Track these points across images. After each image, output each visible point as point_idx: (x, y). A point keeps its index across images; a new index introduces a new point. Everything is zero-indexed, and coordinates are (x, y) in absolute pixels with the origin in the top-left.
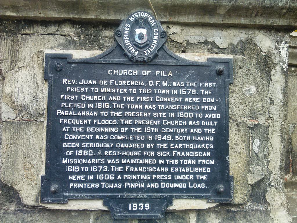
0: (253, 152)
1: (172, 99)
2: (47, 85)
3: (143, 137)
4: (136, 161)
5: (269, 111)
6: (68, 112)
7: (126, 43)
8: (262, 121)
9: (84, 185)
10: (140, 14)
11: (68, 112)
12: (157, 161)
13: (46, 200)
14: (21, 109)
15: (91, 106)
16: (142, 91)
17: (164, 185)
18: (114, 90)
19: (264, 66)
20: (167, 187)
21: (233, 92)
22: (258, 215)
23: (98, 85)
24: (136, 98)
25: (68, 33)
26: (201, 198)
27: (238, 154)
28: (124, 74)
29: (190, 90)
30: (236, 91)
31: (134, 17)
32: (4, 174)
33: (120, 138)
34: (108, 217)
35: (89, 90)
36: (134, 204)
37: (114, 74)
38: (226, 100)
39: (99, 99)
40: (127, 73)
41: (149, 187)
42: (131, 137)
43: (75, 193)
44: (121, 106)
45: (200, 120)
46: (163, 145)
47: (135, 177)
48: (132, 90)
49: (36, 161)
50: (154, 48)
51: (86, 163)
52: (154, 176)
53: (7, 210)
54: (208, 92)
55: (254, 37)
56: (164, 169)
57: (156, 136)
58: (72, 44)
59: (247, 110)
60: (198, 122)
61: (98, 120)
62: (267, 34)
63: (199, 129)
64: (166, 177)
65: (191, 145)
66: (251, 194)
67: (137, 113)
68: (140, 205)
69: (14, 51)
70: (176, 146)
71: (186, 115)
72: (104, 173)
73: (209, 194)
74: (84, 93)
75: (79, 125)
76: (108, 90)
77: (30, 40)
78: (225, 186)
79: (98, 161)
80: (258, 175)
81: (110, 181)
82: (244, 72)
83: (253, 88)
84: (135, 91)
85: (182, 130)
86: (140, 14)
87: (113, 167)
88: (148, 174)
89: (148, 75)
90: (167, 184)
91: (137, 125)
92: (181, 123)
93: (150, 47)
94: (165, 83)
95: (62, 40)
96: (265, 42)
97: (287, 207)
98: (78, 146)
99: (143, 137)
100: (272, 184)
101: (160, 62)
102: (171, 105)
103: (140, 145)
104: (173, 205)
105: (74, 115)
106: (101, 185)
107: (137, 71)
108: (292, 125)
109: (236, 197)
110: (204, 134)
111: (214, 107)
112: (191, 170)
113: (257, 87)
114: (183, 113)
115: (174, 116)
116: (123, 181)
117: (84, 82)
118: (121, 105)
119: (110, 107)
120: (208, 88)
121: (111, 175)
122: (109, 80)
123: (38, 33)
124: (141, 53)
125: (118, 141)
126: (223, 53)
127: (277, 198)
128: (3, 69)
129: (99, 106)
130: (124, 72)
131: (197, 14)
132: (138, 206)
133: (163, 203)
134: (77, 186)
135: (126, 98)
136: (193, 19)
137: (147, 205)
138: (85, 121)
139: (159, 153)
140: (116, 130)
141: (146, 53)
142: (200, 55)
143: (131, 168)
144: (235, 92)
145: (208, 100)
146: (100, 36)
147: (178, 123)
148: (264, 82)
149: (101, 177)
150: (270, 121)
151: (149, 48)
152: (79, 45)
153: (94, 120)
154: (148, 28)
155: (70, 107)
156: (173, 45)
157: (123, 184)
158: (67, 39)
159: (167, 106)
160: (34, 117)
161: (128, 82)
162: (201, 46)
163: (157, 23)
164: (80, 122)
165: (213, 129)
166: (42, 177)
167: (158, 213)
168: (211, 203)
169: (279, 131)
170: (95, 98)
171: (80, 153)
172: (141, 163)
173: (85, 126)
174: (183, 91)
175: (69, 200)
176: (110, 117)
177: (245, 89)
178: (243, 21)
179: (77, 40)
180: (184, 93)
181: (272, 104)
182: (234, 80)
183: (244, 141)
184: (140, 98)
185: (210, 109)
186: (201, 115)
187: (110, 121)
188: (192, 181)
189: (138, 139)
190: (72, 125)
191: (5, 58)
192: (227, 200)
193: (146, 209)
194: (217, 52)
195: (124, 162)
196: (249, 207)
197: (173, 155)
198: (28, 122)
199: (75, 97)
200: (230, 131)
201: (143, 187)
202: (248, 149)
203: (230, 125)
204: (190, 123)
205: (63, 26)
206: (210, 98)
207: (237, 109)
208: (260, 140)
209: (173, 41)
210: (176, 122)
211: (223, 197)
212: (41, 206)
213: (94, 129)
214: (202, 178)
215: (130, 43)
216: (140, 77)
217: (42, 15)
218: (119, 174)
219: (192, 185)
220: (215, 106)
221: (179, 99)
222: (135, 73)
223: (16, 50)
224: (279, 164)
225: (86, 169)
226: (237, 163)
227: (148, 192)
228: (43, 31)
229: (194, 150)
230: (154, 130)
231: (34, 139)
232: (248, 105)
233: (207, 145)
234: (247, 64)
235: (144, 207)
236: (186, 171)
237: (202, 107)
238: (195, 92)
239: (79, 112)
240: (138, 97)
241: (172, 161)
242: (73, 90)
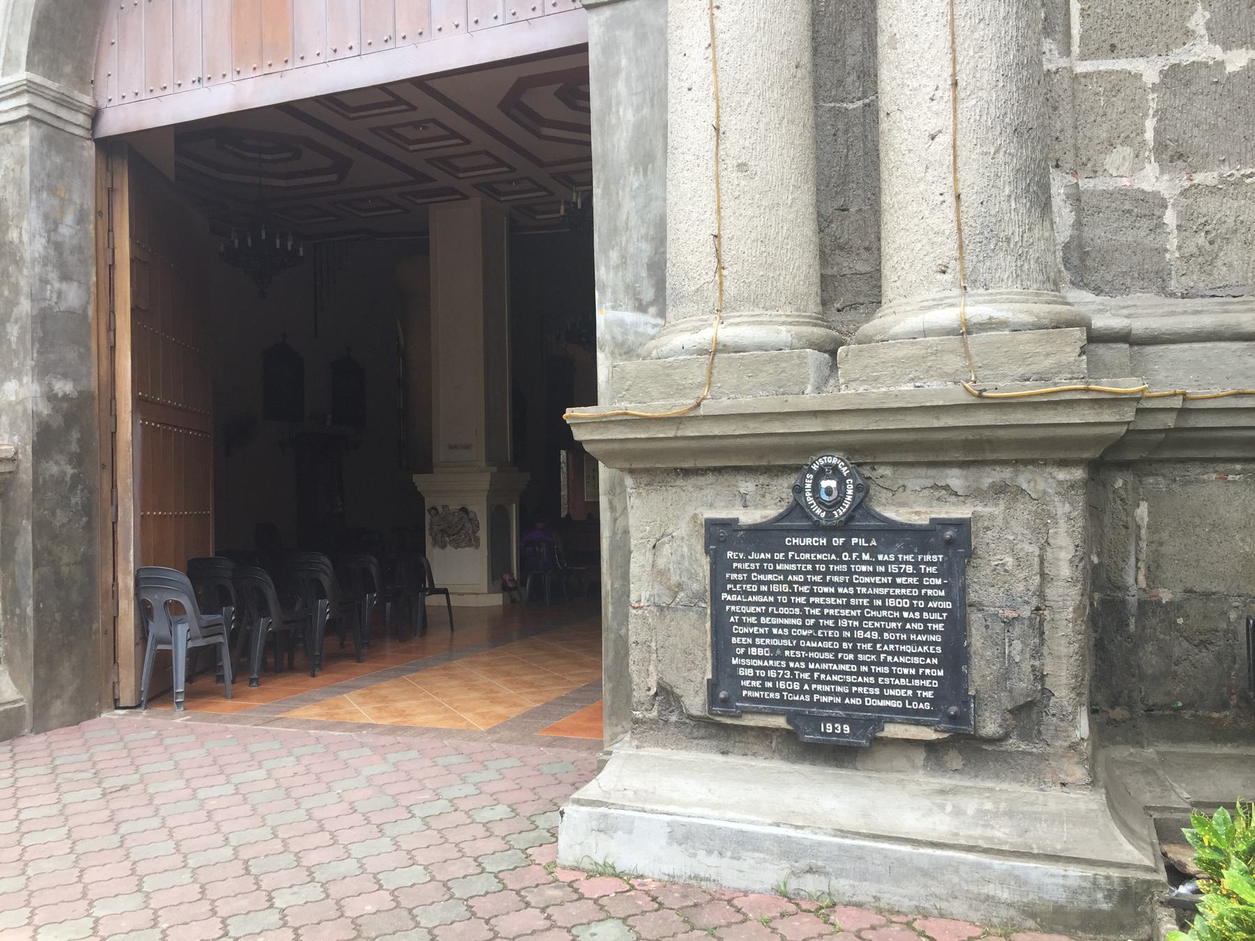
15: (764, 588)
17: (870, 702)
18: (793, 567)
33: (804, 633)
44: (805, 589)
45: (921, 611)
47: (827, 688)
52: (854, 689)
54: (932, 570)
60: (917, 614)
70: (886, 648)
75: (751, 615)
76: (787, 567)
81: (793, 691)
84: (823, 568)
85: (893, 625)
91: (828, 617)
106: (782, 696)
110: (926, 631)
116: (812, 693)
117: (754, 556)
124: (830, 515)
125: (802, 637)
130: (808, 541)
138: (758, 610)
140: (798, 622)
149: (782, 685)
157: (812, 698)
164: (752, 609)
170: (770, 577)
171: (753, 651)
173: (758, 615)
174: (893, 568)
176: (790, 604)
186: (921, 604)
190: (742, 614)
195: (811, 666)
204: (906, 615)
210: (884, 613)
216: (829, 548)
219: (910, 704)
229: (913, 655)
241: (880, 669)
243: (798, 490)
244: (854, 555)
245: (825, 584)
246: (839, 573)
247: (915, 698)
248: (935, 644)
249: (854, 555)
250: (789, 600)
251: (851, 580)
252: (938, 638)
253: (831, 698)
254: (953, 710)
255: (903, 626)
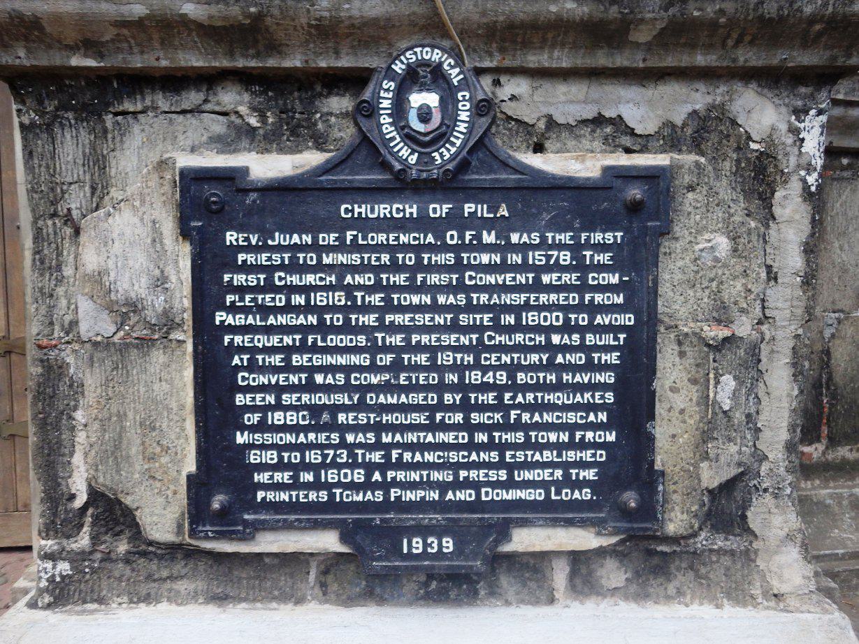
0: (717, 407)
1: (508, 279)
2: (186, 249)
3: (434, 378)
4: (419, 437)
5: (763, 300)
6: (243, 316)
7: (385, 131)
8: (743, 328)
9: (291, 496)
10: (422, 52)
11: (243, 316)
12: (471, 437)
13: (202, 531)
14: (127, 310)
15: (298, 300)
16: (430, 259)
17: (488, 494)
18: (355, 259)
19: (754, 179)
20: (496, 498)
21: (670, 254)
22: (726, 561)
23: (315, 247)
24: (412, 279)
25: (232, 106)
26: (583, 524)
27: (677, 414)
28: (382, 216)
29: (555, 253)
30: (678, 251)
31: (405, 62)
32: (97, 470)
33: (375, 380)
34: (352, 567)
35: (294, 259)
36: (415, 540)
37: (356, 216)
38: (650, 277)
39: (319, 283)
40: (391, 212)
41: (450, 500)
42: (403, 376)
43: (271, 515)
45: (582, 330)
46: (485, 397)
47: (414, 476)
48: (404, 258)
49: (173, 437)
50: (458, 143)
51: (294, 442)
52: (463, 474)
53: (109, 553)
54: (604, 258)
55: (731, 100)
56: (490, 457)
57: (467, 373)
58: (240, 136)
59: (706, 300)
60: (576, 337)
61: (319, 337)
62: (766, 91)
63: (578, 355)
64: (493, 475)
65: (557, 394)
66: (710, 510)
67: (417, 317)
68: (429, 541)
69: (98, 160)
70: (520, 399)
71: (545, 318)
72: (340, 467)
73: (601, 515)
74: (282, 267)
76: (342, 259)
77: (136, 129)
78: (641, 495)
79: (322, 438)
80: (729, 465)
82: (700, 199)
83: (723, 243)
85: (534, 358)
86: (422, 52)
87: (360, 452)
88: (449, 468)
89: (444, 215)
90: (496, 491)
91: (419, 348)
92: (531, 339)
93: (448, 141)
94: (489, 234)
95: (218, 126)
96: (760, 115)
97: (803, 542)
98: (273, 403)
99: (434, 378)
100: (764, 486)
101: (476, 180)
102: (506, 293)
103: (426, 398)
104: (511, 540)
105: (259, 323)
106: (332, 496)
107: (415, 206)
108: (833, 315)
109: (671, 520)
110: (590, 366)
111: (618, 296)
112: (557, 457)
113: (734, 239)
114: (536, 313)
115: (513, 323)
116: (386, 486)
117: (278, 239)
118: (377, 296)
119: (349, 303)
120: (601, 248)
121: (356, 471)
122: (342, 232)
123: (155, 108)
124: (426, 159)
125: (371, 388)
126: (644, 150)
127: (777, 520)
128: (73, 206)
129: (321, 301)
130: (383, 210)
131: (575, 47)
132: (426, 545)
133: (487, 536)
134: (274, 497)
135: (388, 279)
136: (562, 59)
137: (448, 542)
138: (288, 340)
139: (476, 418)
140: (362, 360)
141: (438, 157)
142: (582, 159)
143: (405, 454)
144: (673, 256)
145: (604, 278)
146: (316, 112)
147: (524, 340)
148: (753, 224)
149: (331, 476)
150: (764, 328)
151: (447, 145)
152: (264, 139)
153: (310, 337)
154: (444, 90)
155: (247, 304)
156: (510, 130)
158: (233, 122)
159: (495, 296)
160: (160, 329)
161: (392, 237)
162: (586, 131)
163: (468, 76)
164: (274, 341)
165: (614, 354)
166: (189, 477)
167: (475, 560)
168: (605, 535)
169: (788, 352)
170: (310, 279)
171: (278, 418)
172: (430, 443)
173: (288, 351)
174: (537, 258)
175: (257, 530)
176: (347, 328)
177: (701, 246)
178: (701, 59)
179: (259, 125)
180: (541, 260)
181: (772, 283)
182: (672, 221)
183: (694, 381)
184: (425, 278)
185: (606, 303)
187: (349, 337)
188: (559, 486)
189: (421, 382)
190: (253, 351)
191: (75, 179)
192: (647, 529)
193: (445, 550)
194: (628, 145)
195: (386, 439)
196: (704, 542)
197: (512, 422)
198: (145, 344)
199: (258, 279)
200: (659, 356)
201: (437, 498)
202: (705, 400)
203: (659, 340)
204: (556, 339)
205: (219, 89)
206: (608, 273)
207: (678, 300)
208: (735, 378)
209: (509, 118)
210: (519, 338)
211: (636, 522)
212: (191, 545)
213: (310, 360)
214: (584, 477)
215: (395, 133)
216: (422, 223)
217: (164, 63)
218: (377, 469)
219: (558, 493)
220: (622, 295)
221: (527, 278)
222: (411, 210)
223: (103, 156)
224: (784, 435)
225: (296, 457)
226: (674, 436)
227: (449, 512)
228: (169, 103)
230: (462, 359)
231: (163, 383)
232: (707, 288)
233: (597, 394)
234: (709, 177)
235: (440, 545)
236: (545, 460)
237: (587, 297)
238: (568, 258)
239: (272, 317)
240: (419, 276)
241: (509, 437)
242: (253, 260)
243: (368, 111)
244: (468, 236)
245: (413, 288)
246: (440, 269)
247: (568, 482)
248: (604, 387)
249: (468, 236)
250: (347, 321)
251: (461, 280)
252: (608, 378)
253: (421, 493)
254: (631, 499)
255: (551, 360)
